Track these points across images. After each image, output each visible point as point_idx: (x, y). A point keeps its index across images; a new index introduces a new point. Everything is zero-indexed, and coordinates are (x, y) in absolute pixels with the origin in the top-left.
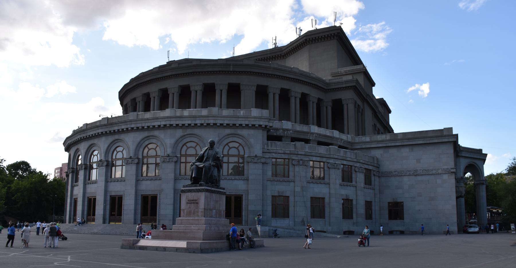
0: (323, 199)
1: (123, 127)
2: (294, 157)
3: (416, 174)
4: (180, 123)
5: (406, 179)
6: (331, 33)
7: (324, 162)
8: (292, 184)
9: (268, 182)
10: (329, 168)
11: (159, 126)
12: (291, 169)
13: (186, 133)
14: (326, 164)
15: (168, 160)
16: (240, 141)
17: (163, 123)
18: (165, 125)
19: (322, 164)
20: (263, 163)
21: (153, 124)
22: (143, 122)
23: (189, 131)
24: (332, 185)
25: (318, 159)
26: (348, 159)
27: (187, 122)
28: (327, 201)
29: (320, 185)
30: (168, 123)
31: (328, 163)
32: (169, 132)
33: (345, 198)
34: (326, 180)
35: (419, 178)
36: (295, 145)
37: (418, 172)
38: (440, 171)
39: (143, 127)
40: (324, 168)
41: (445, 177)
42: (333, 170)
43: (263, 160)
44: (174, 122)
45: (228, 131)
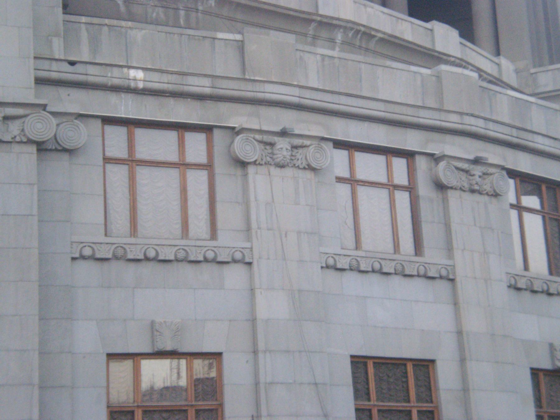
0: (425, 366)
2: (239, 117)
7: (409, 155)
8: (235, 276)
9: (82, 265)
10: (441, 187)
12: (227, 185)
14: (421, 163)
19: (400, 164)
20: (41, 147)
24: (467, 288)
25: (379, 136)
26: (542, 144)
28: (446, 377)
29: (396, 280)
31: (435, 159)
33: (546, 364)
34: (434, 256)
36: (241, 47)
40: (411, 189)
42: (467, 196)
43: (41, 127)
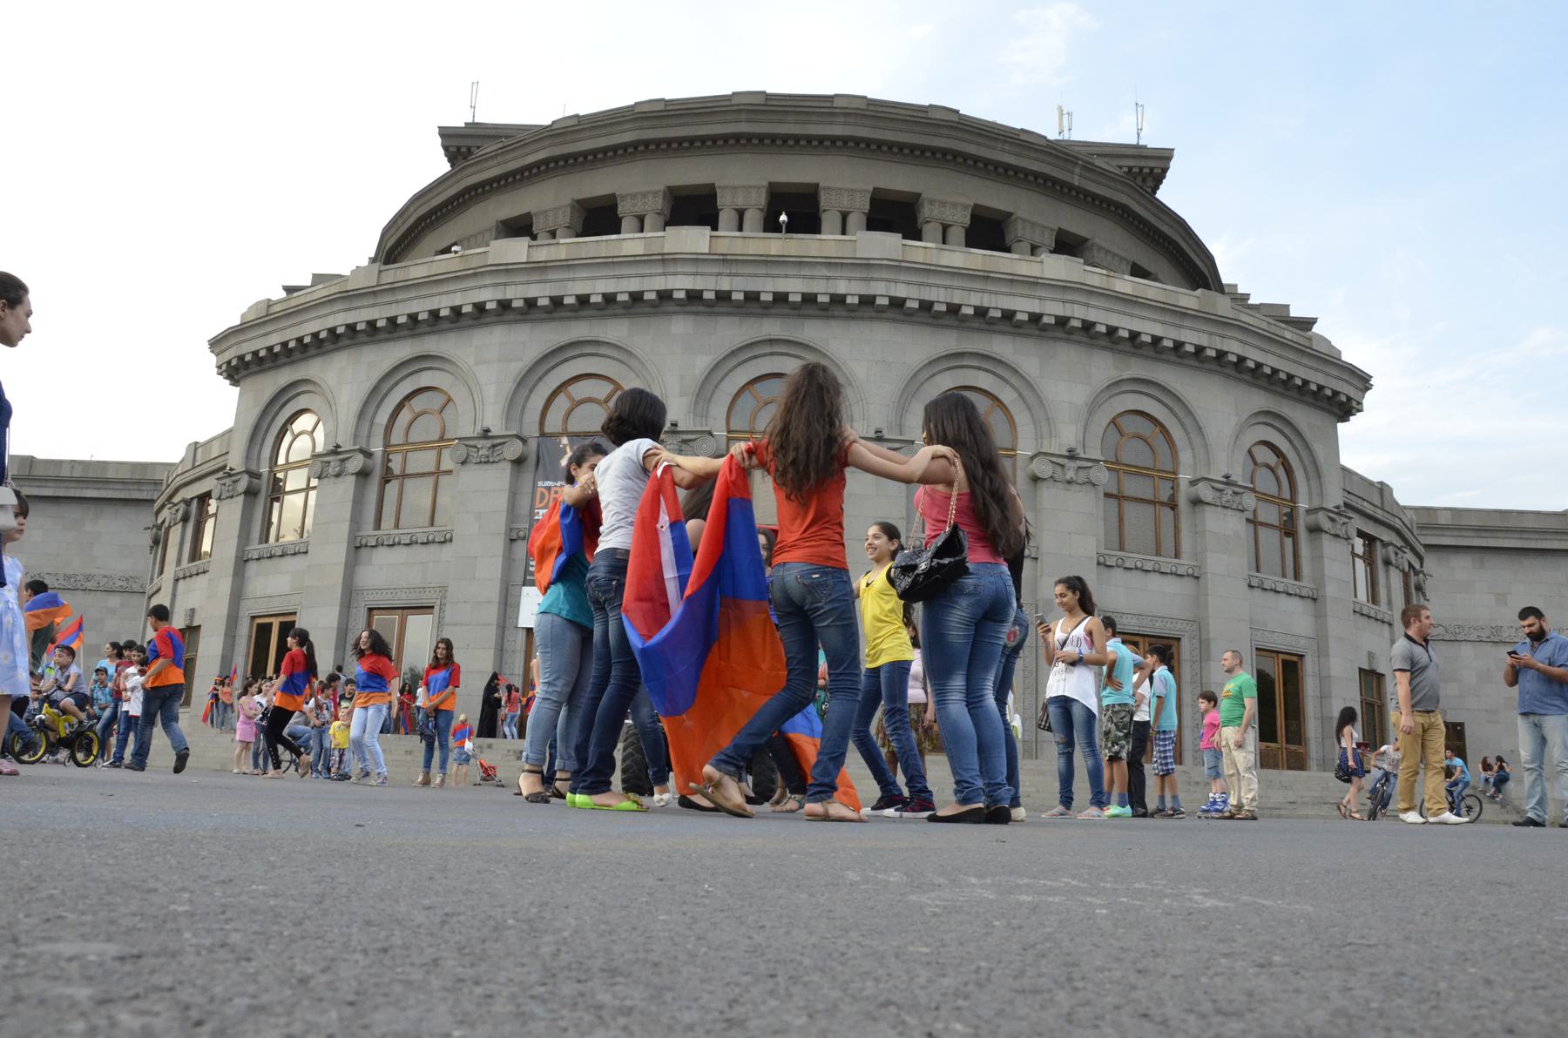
1: (841, 287)
4: (1126, 323)
5: (1466, 651)
6: (1142, 163)
11: (1035, 318)
13: (1127, 375)
15: (1070, 474)
16: (1284, 446)
17: (1052, 309)
18: (1062, 322)
27: (1149, 328)
30: (1078, 313)
32: (1067, 355)
39: (954, 309)
44: (1103, 318)
45: (1260, 400)
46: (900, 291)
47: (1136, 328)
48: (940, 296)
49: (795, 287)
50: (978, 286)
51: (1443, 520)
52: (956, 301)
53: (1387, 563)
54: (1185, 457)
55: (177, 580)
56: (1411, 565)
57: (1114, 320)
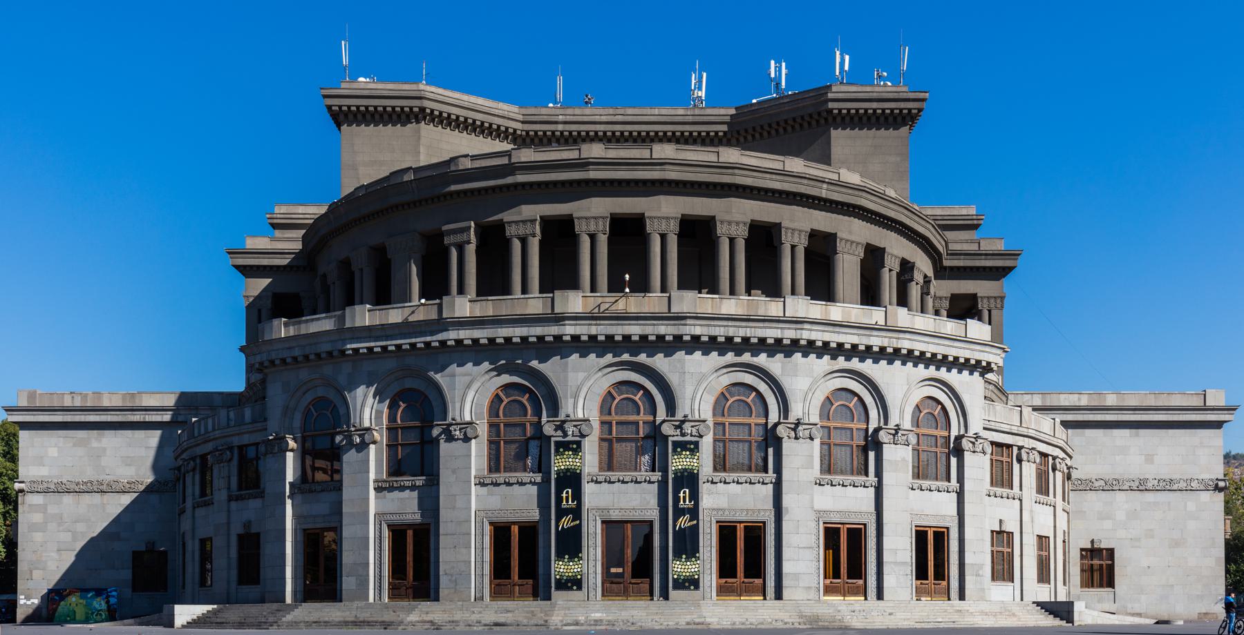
3: (1142, 487)
4: (834, 338)
13: (836, 368)
21: (761, 333)
22: (730, 323)
23: (841, 362)
27: (848, 339)
35: (1150, 497)
37: (1150, 485)
38: (1195, 485)
41: (1206, 496)
45: (922, 371)
46: (697, 331)
47: (841, 341)
48: (720, 331)
49: (635, 330)
50: (744, 324)
51: (1111, 400)
52: (731, 334)
53: (1020, 461)
54: (873, 413)
55: (230, 499)
56: (1044, 455)
57: (827, 337)
